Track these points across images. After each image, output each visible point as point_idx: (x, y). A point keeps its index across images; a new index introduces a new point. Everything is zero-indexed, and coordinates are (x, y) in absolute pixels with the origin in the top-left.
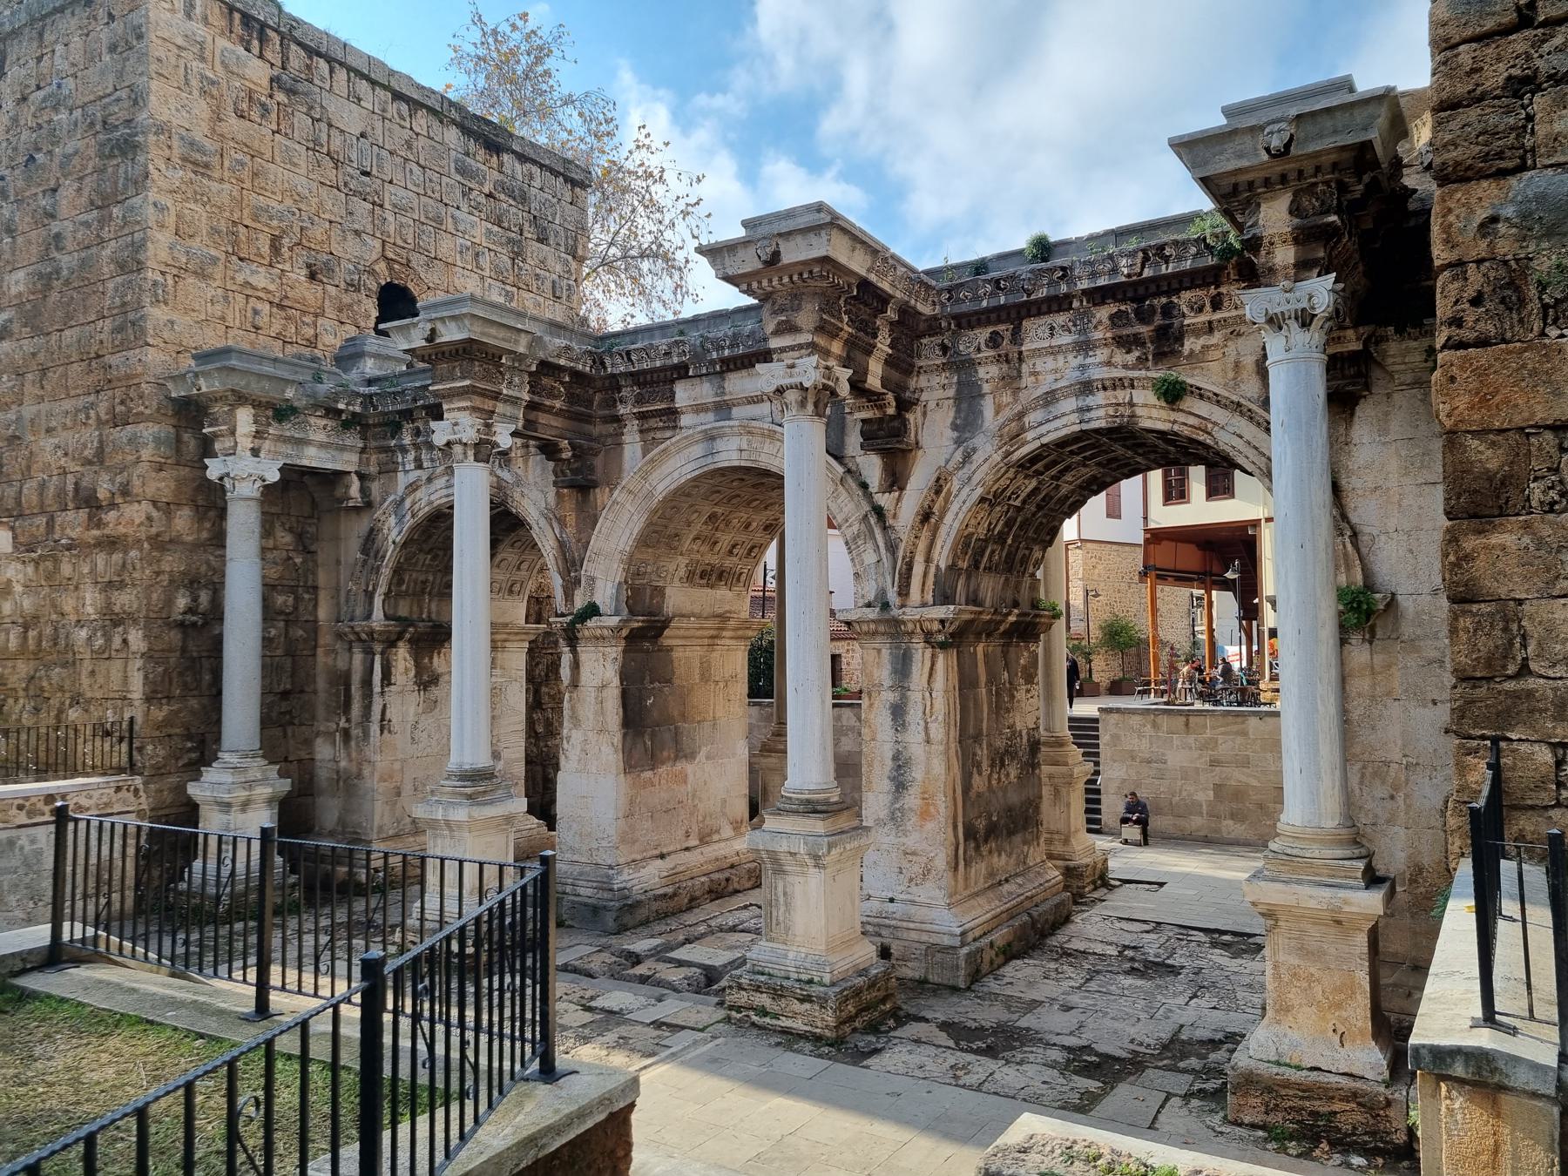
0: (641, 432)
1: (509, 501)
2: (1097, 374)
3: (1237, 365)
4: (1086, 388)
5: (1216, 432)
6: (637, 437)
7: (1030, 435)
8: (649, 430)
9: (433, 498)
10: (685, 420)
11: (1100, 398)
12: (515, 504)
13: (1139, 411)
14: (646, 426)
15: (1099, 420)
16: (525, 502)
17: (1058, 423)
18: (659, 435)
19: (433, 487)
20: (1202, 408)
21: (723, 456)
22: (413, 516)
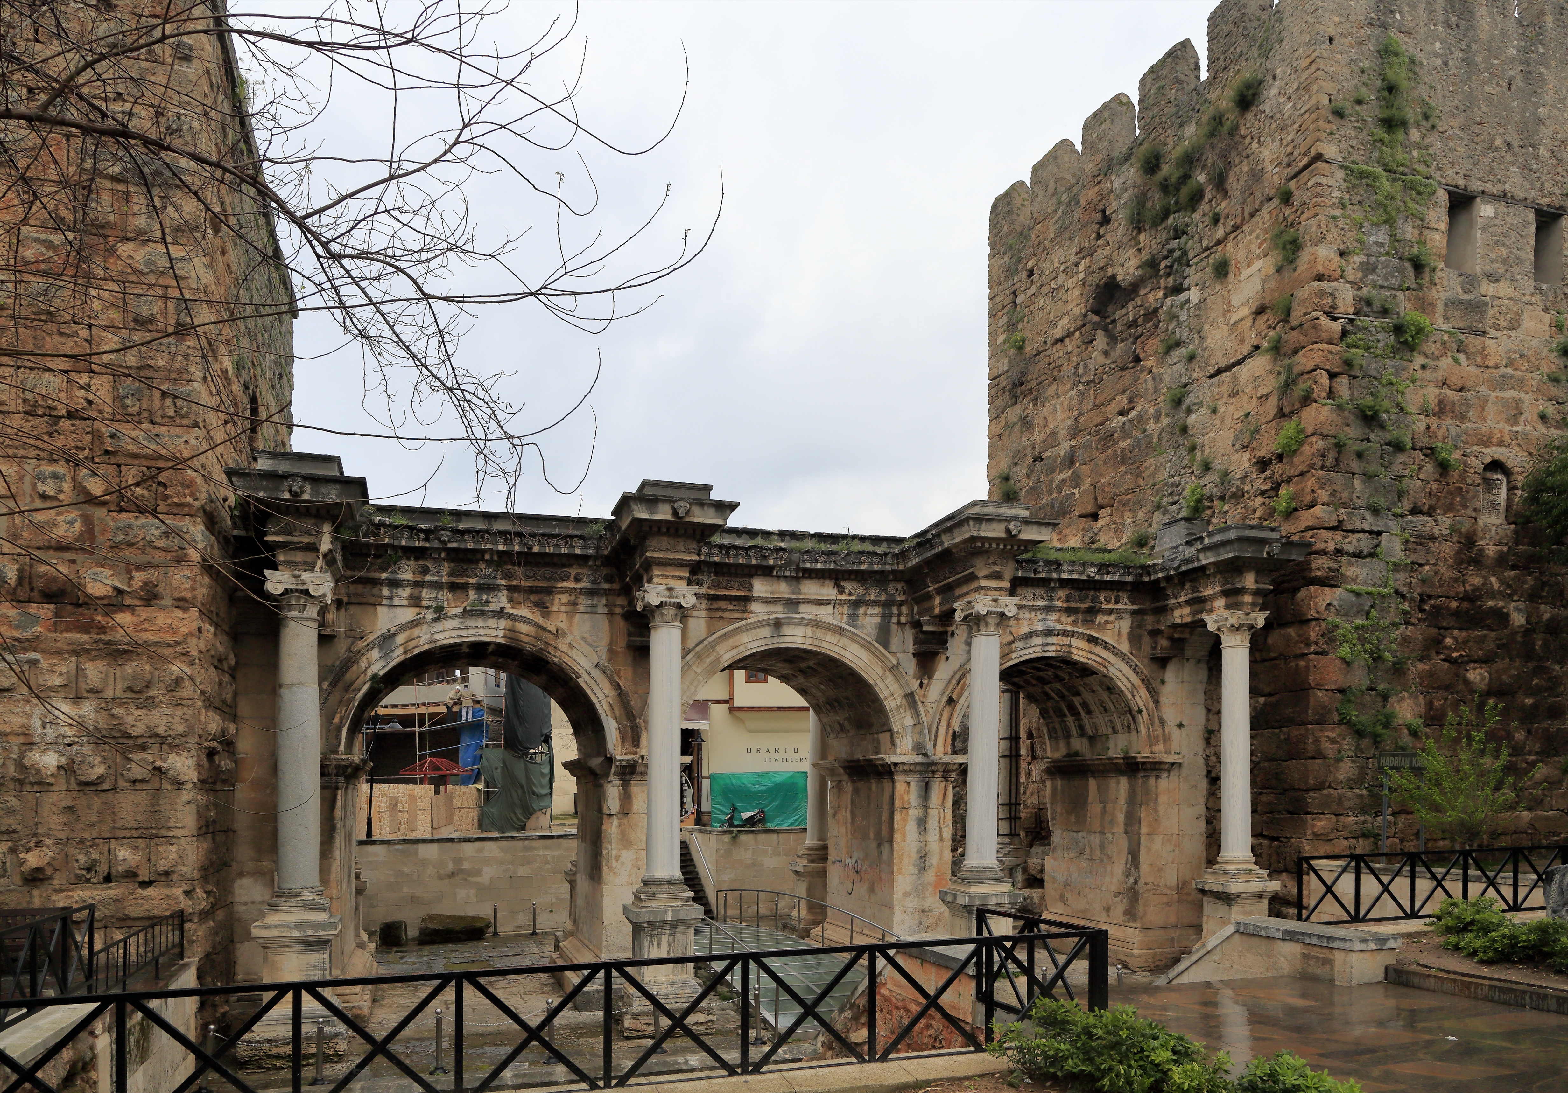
0: (709, 610)
1: (551, 650)
2: (1058, 626)
3: (1119, 633)
4: (1049, 632)
5: (1111, 669)
6: (703, 614)
7: (1014, 655)
8: (717, 610)
9: (436, 637)
10: (754, 607)
11: (1054, 640)
12: (558, 654)
13: (1073, 650)
14: (715, 606)
15: (1051, 652)
16: (574, 654)
17: (1030, 650)
18: (727, 615)
19: (438, 627)
20: (1105, 654)
21: (787, 639)
22: (405, 652)
